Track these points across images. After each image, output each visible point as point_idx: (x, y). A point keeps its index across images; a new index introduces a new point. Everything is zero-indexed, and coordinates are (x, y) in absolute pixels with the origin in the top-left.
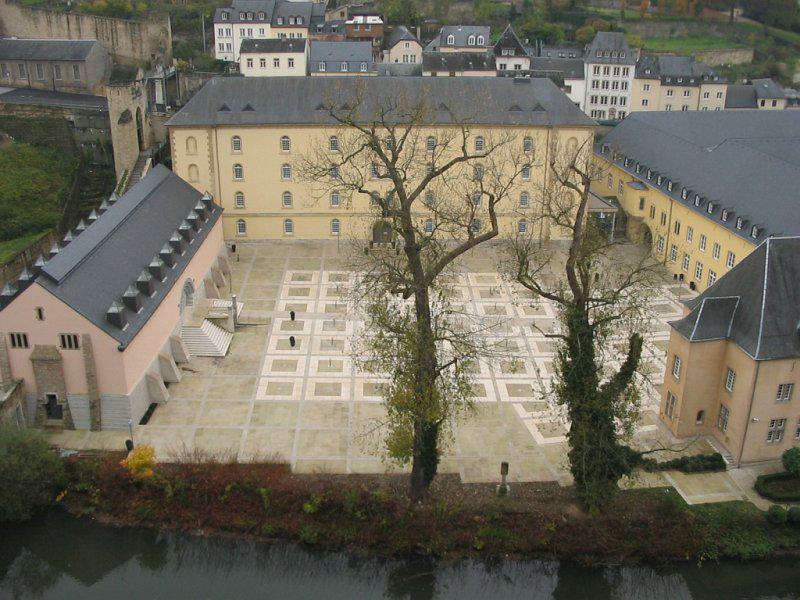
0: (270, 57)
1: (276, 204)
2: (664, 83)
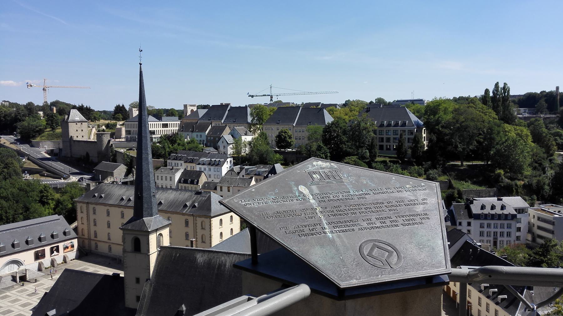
1: (106, 239)
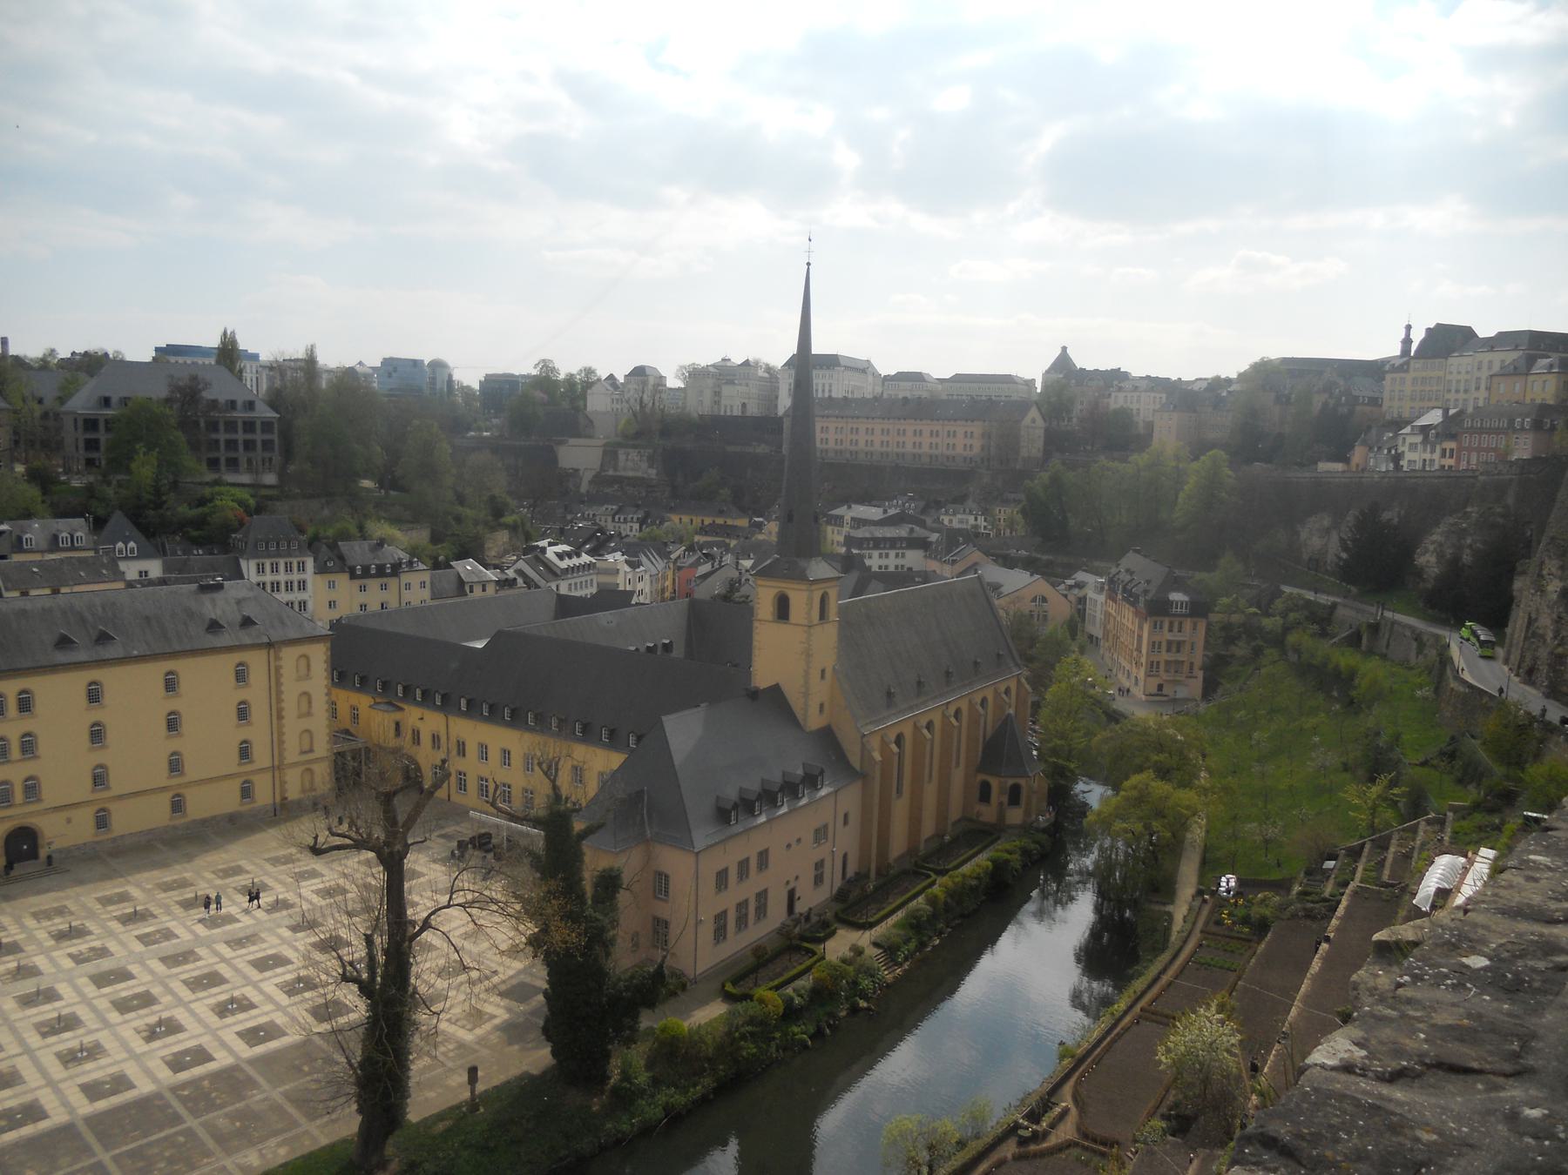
2: (353, 576)
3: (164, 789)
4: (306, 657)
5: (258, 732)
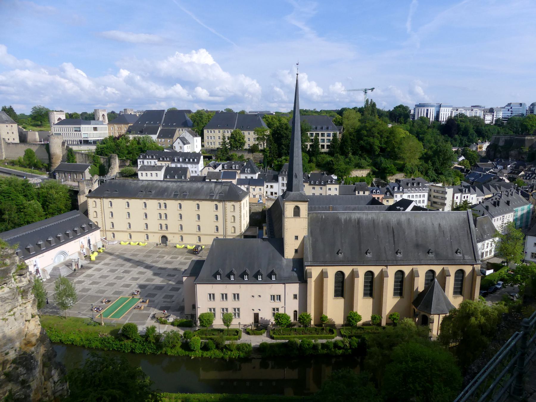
0: (149, 173)
2: (310, 184)
3: (195, 234)
4: (234, 205)
5: (220, 224)
